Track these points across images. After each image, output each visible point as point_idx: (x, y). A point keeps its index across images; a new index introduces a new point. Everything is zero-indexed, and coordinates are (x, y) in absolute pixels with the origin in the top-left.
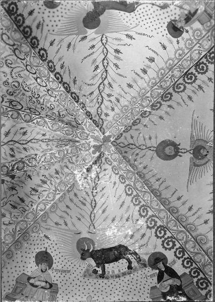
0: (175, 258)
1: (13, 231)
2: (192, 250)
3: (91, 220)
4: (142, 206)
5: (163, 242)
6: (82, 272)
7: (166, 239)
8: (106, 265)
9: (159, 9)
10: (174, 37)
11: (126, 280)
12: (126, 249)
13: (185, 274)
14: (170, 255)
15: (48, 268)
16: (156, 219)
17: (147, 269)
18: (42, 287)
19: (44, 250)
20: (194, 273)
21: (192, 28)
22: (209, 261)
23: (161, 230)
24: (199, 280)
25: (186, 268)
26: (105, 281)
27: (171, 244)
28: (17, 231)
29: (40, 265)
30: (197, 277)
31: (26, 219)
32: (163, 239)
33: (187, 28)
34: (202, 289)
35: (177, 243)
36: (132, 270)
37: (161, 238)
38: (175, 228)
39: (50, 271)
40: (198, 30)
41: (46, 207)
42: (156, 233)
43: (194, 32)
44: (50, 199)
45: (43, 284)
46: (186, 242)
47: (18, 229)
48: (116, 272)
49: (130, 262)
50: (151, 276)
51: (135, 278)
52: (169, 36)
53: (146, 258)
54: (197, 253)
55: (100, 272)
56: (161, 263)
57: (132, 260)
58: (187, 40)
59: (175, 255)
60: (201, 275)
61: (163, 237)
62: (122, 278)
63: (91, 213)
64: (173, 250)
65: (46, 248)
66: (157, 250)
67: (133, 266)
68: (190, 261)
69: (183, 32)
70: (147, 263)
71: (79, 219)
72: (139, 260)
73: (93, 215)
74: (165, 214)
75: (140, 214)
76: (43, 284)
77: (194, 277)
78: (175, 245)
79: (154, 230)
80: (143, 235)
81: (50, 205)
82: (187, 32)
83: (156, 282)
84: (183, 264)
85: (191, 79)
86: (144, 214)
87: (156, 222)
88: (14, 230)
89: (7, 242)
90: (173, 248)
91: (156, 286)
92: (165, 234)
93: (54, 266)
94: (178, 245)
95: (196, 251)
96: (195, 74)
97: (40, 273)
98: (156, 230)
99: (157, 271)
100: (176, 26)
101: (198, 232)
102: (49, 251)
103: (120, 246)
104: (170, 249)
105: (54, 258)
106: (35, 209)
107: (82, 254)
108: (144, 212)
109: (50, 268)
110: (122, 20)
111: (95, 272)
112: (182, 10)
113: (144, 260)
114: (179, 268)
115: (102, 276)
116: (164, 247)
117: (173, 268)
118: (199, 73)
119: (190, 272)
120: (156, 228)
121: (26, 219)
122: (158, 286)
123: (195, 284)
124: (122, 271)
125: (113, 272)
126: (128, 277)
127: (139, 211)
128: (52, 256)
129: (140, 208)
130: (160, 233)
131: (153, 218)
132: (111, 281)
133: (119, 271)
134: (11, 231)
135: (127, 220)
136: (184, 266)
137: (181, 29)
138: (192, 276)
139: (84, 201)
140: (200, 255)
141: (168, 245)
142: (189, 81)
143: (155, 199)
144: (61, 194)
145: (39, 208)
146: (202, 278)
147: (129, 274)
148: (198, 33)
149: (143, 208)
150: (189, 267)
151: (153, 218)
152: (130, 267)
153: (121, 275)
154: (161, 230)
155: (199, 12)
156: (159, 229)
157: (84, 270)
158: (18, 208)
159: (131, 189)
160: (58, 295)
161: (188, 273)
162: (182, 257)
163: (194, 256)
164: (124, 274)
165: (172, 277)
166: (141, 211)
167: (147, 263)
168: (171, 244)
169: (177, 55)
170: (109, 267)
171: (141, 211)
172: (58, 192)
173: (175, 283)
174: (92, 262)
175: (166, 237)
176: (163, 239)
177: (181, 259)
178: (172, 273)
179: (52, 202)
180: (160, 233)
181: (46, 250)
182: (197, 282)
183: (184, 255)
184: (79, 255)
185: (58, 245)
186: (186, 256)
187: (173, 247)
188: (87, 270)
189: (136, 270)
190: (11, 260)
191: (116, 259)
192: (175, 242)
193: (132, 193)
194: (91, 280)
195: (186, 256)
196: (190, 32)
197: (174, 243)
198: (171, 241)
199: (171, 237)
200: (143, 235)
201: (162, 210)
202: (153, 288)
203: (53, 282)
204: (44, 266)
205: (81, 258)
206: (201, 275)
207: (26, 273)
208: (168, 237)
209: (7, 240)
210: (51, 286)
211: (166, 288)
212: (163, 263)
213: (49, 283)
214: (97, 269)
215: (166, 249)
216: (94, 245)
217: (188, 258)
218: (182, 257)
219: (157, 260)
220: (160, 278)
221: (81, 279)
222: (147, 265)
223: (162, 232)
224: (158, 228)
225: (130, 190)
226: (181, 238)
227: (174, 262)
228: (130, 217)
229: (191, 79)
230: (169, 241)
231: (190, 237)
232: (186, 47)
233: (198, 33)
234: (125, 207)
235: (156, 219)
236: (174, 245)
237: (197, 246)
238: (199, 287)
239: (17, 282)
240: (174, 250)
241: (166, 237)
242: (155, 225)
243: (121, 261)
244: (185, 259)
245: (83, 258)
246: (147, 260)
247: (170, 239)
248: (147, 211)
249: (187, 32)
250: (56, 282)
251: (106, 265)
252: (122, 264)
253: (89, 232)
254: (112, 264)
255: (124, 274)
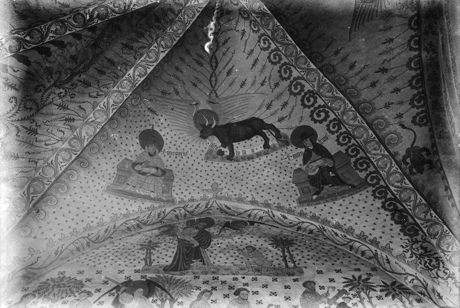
0: (328, 134)
1: (104, 106)
2: (351, 122)
3: (211, 85)
4: (283, 65)
5: (312, 112)
6: (204, 154)
7: (316, 109)
8: (235, 144)
11: (261, 162)
12: (261, 121)
13: (340, 152)
14: (320, 130)
15: (157, 151)
16: (303, 82)
17: (290, 148)
18: (153, 175)
19: (150, 128)
20: (352, 151)
22: (374, 136)
23: (310, 96)
24: (357, 160)
25: (342, 145)
26: (235, 164)
27: (323, 115)
28: (110, 105)
29: (146, 147)
30: (355, 156)
31: (120, 89)
32: (312, 109)
34: (361, 171)
35: (331, 114)
36: (270, 150)
37: (309, 107)
38: (330, 94)
39: (160, 155)
41: (146, 71)
42: (302, 100)
44: (151, 60)
45: (154, 171)
46: (344, 113)
47: (111, 102)
48: (249, 152)
49: (266, 140)
50: (295, 156)
51: (274, 158)
53: (289, 133)
54: (357, 127)
55: (227, 153)
56: (308, 140)
57: (269, 137)
59: (328, 129)
60: (362, 154)
61: (313, 105)
62: (257, 160)
63: (211, 76)
64: (325, 123)
65: (153, 125)
66: (302, 124)
67: (270, 144)
68: (347, 137)
70: (289, 140)
71: (195, 85)
72: (278, 136)
73: (213, 79)
74: (316, 75)
75: (281, 76)
76: (154, 171)
77: (352, 156)
78: (329, 116)
79: (299, 98)
80: (285, 104)
81: (152, 68)
83: (302, 162)
84: (338, 140)
86: (286, 76)
87: (303, 87)
88: (106, 104)
89: (98, 120)
90: (326, 120)
91: (300, 169)
92: (315, 102)
93: (165, 147)
94: (332, 116)
95: (356, 123)
97: (148, 158)
98: (303, 97)
99: (303, 150)
101: (362, 98)
102: (156, 129)
103: (253, 119)
104: (321, 122)
105: (164, 138)
106: (131, 75)
107: (202, 132)
108: (285, 72)
109: (160, 150)
111: (221, 153)
113: (286, 137)
114: (332, 146)
115: (231, 158)
116: (313, 119)
117: (323, 145)
119: (347, 150)
120: (303, 94)
121: (120, 89)
122: (304, 168)
123: (352, 165)
124: (256, 151)
125: (245, 152)
126: (264, 158)
127: (280, 72)
128: (162, 135)
129: (281, 68)
130: (309, 101)
131: (299, 81)
132: (242, 163)
133: (253, 151)
134: (102, 106)
135: (262, 84)
136: (339, 143)
138: (349, 155)
139: (200, 60)
140: (362, 129)
141: (319, 116)
143: (303, 54)
144: (167, 52)
145: (137, 73)
146: (362, 158)
147: (266, 154)
149: (284, 67)
150: (346, 144)
151: (299, 81)
152: (266, 146)
153: (255, 156)
154: (310, 96)
156: (308, 96)
157: (206, 151)
158: (107, 73)
159: (268, 41)
160: (174, 184)
161: (344, 152)
162: (337, 132)
163: (353, 131)
164: (259, 155)
165: (322, 157)
166: (283, 71)
167: (289, 140)
168: (323, 115)
170: (240, 148)
171: (283, 71)
172: (162, 49)
173: (326, 164)
174: (216, 141)
175: (316, 105)
176: (312, 109)
177: (336, 134)
178: (322, 152)
179: (155, 64)
180: (309, 101)
181: (153, 128)
182: (355, 163)
183: (340, 128)
184: (198, 133)
185: (168, 121)
186: (343, 130)
187: (325, 119)
188: (210, 152)
189: (274, 149)
190: (107, 143)
191: (248, 137)
192: (328, 112)
193: (269, 47)
194: (215, 164)
195: (343, 130)
197: (326, 113)
198: (323, 111)
199: (324, 106)
200: (285, 104)
201: (313, 70)
202: (299, 170)
203: (165, 168)
204: (151, 149)
205: (201, 136)
206: (362, 154)
207: (130, 158)
208: (320, 107)
209: (98, 118)
210: (164, 172)
211: (314, 171)
212: (311, 140)
213: (161, 169)
214: (223, 149)
215: (316, 121)
216: (217, 120)
217: (345, 132)
218: (337, 132)
219: (303, 135)
220: (307, 158)
221: (203, 163)
222: (290, 143)
223: (312, 99)
224: (306, 94)
225: (267, 42)
226: (337, 107)
227: (326, 138)
228: (267, 80)
230: (320, 111)
231: (350, 105)
234: (259, 66)
235: (303, 82)
236: (327, 116)
237: (359, 118)
238: (357, 169)
239: (118, 170)
240: (327, 122)
241: (316, 105)
242: (302, 90)
243: (254, 138)
244: (341, 134)
245: (204, 136)
246: (290, 137)
247: (321, 109)
248: (291, 72)
250: (169, 168)
251: (235, 144)
252: (256, 143)
253: (209, 102)
254: (242, 143)
255: (259, 155)
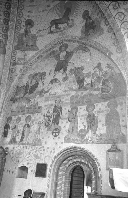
9: (41, 29)
10: (28, 20)
21: (23, 29)
33: (25, 27)
40: (20, 30)
43: (21, 27)
52: (30, 18)
58: (21, 23)
69: (25, 25)
82: (24, 26)
85: (7, 6)
96: (8, 11)
100: (30, 25)
110: (55, 14)
112: (31, 34)
118: (6, 11)
137: (27, 25)
142: (7, 4)
148: (19, 28)
155: (24, 37)
169: (21, 13)
196: (22, 27)
229: (7, 6)
232: (20, 20)
233: (19, 28)
249: (24, 26)
